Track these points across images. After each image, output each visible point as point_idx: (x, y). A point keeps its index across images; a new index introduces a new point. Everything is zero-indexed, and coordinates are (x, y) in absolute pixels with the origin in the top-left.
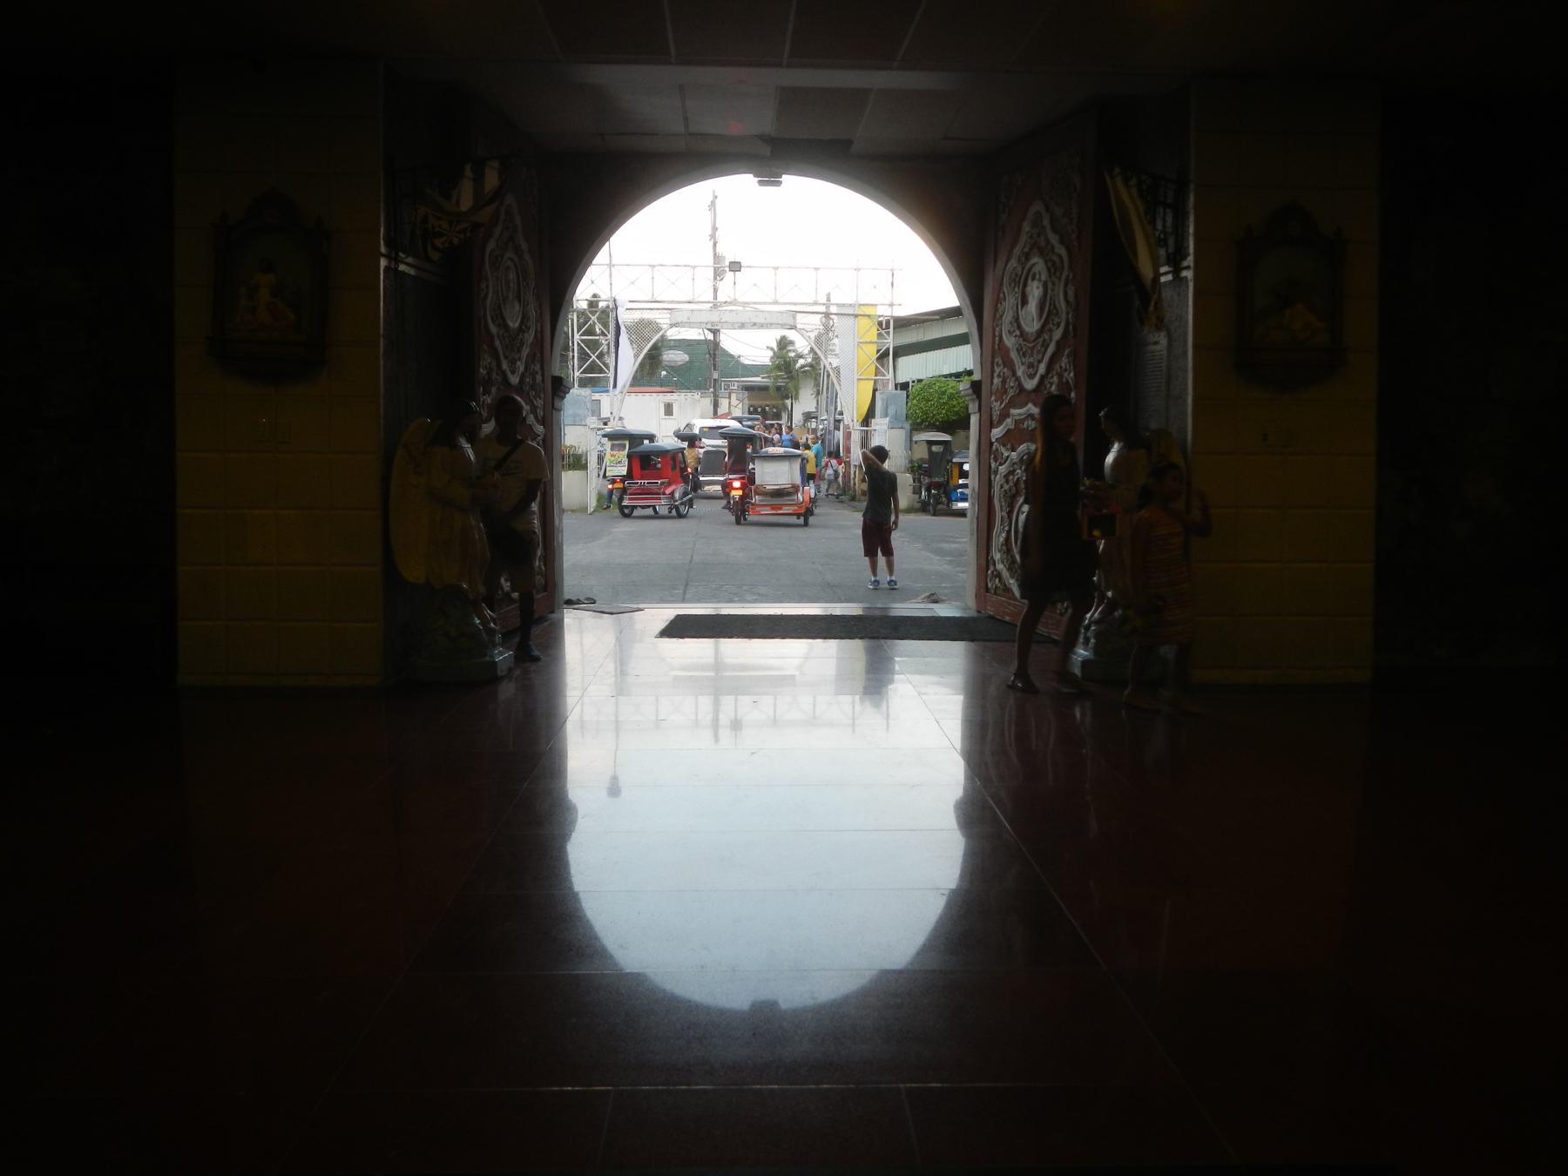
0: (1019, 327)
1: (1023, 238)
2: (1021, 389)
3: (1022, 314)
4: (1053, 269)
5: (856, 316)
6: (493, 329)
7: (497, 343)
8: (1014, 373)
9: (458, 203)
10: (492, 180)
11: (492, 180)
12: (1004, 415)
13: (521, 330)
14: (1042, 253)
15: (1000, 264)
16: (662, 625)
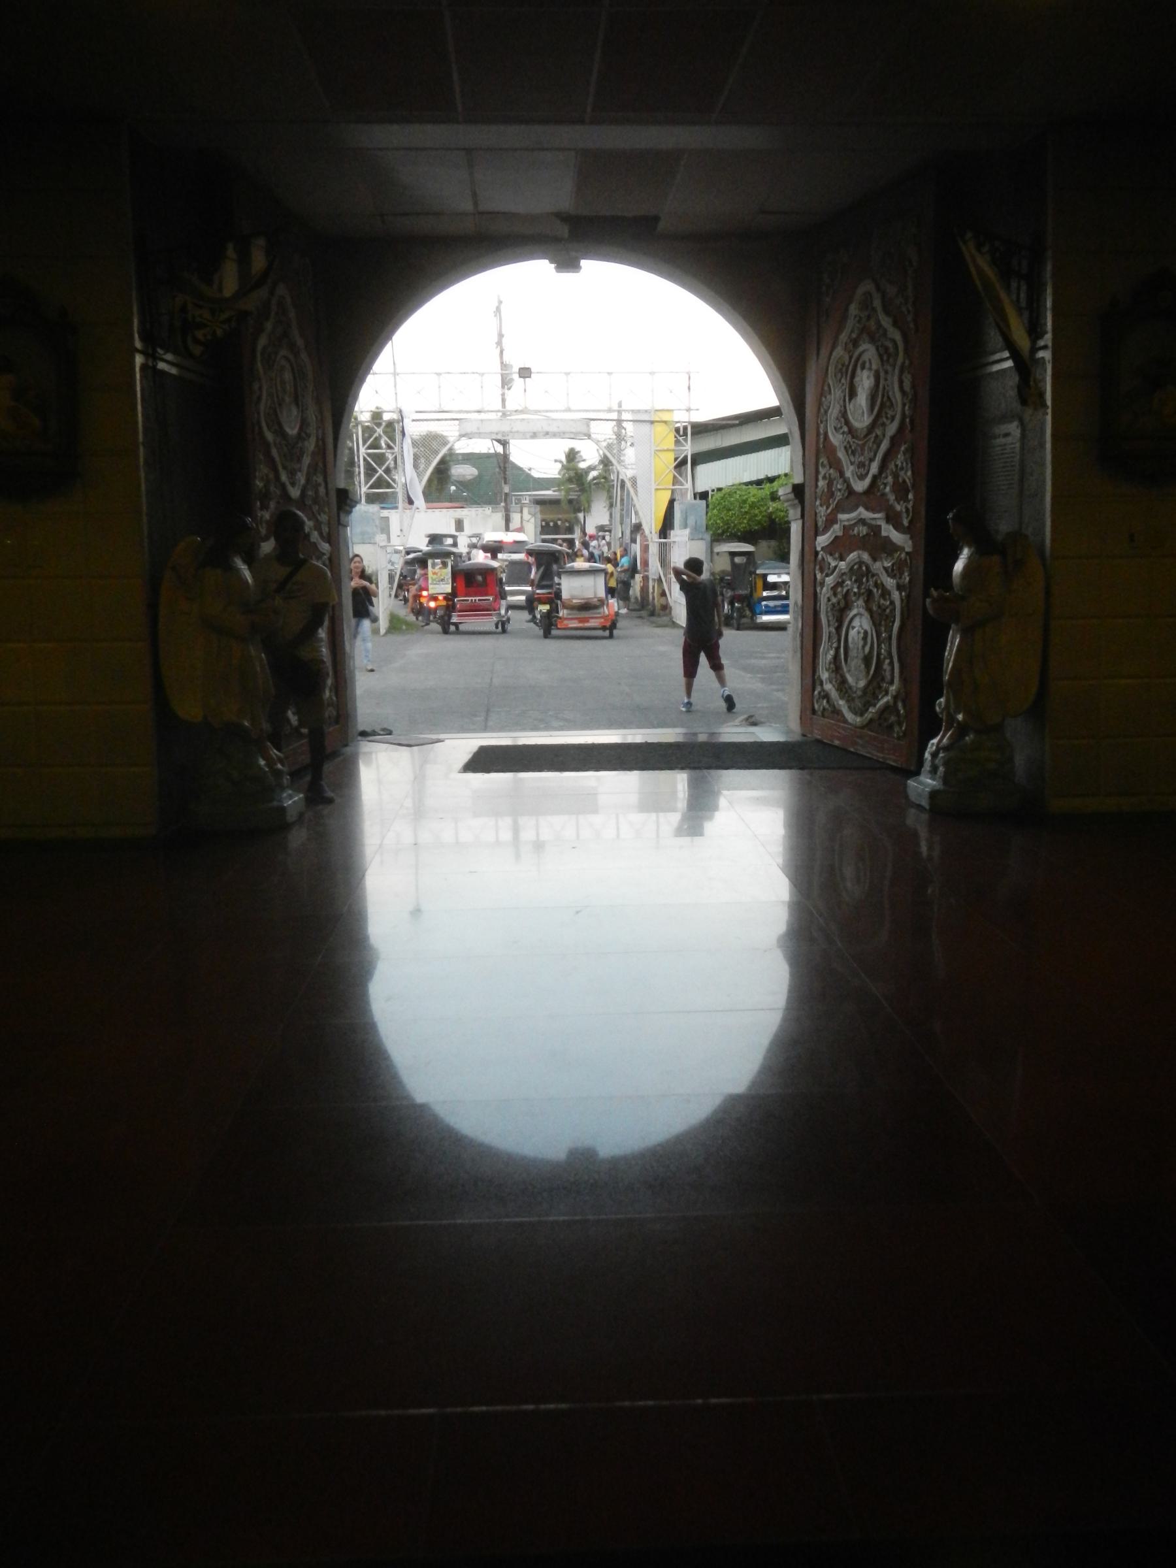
0: (847, 423)
1: (850, 323)
2: (851, 492)
3: (850, 407)
4: (885, 355)
5: (652, 422)
6: (269, 436)
7: (274, 452)
8: (842, 474)
9: (220, 290)
10: (259, 261)
11: (259, 261)
12: (831, 521)
13: (302, 436)
14: (872, 340)
15: (824, 352)
16: (465, 757)
